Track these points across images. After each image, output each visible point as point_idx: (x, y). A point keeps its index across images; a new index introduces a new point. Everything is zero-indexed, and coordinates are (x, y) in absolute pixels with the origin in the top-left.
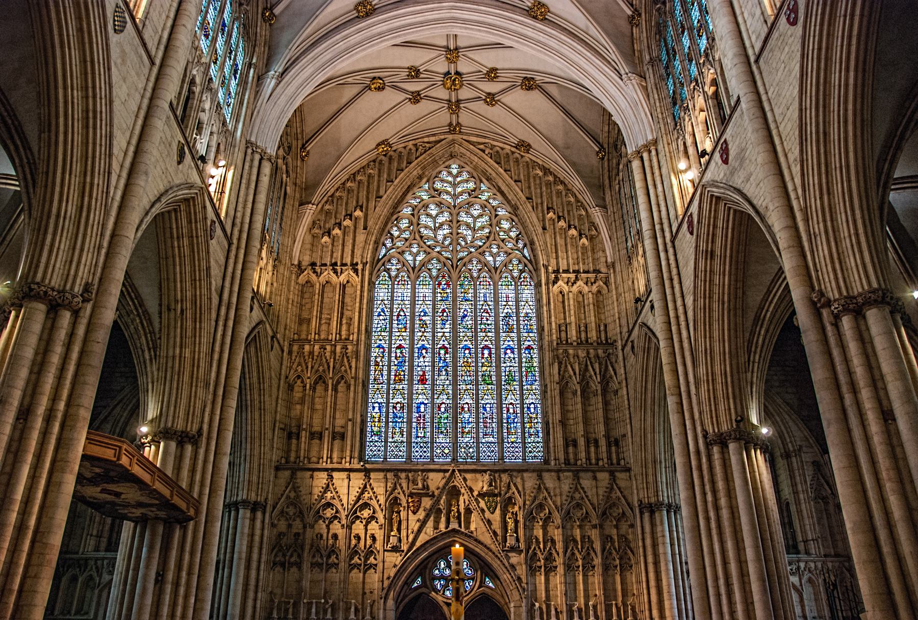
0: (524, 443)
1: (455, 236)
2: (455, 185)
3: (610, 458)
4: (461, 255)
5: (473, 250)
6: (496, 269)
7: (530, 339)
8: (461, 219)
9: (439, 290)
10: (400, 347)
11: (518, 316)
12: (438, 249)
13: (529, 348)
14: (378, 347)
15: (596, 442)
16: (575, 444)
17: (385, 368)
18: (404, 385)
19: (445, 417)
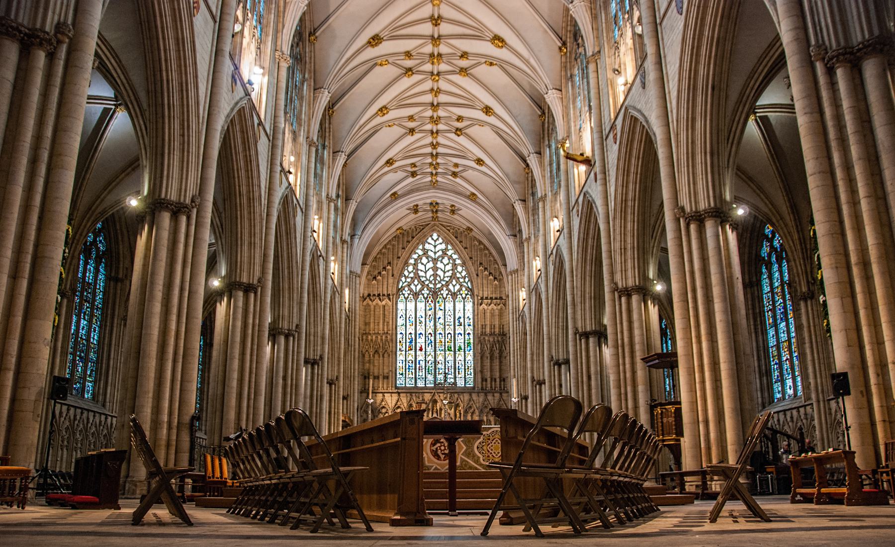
0: (465, 378)
1: (435, 275)
2: (435, 246)
3: (500, 387)
4: (439, 286)
5: (444, 283)
6: (454, 293)
7: (469, 330)
8: (438, 266)
9: (428, 304)
10: (410, 334)
11: (464, 318)
12: (427, 283)
13: (469, 334)
14: (401, 333)
15: (495, 379)
16: (486, 380)
17: (404, 344)
18: (413, 352)
19: (430, 365)
